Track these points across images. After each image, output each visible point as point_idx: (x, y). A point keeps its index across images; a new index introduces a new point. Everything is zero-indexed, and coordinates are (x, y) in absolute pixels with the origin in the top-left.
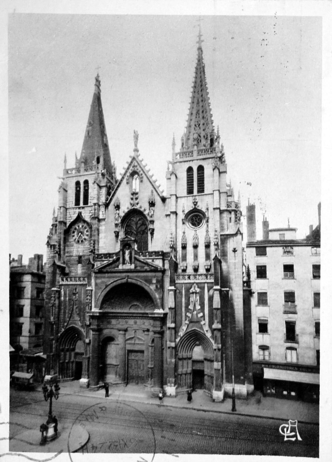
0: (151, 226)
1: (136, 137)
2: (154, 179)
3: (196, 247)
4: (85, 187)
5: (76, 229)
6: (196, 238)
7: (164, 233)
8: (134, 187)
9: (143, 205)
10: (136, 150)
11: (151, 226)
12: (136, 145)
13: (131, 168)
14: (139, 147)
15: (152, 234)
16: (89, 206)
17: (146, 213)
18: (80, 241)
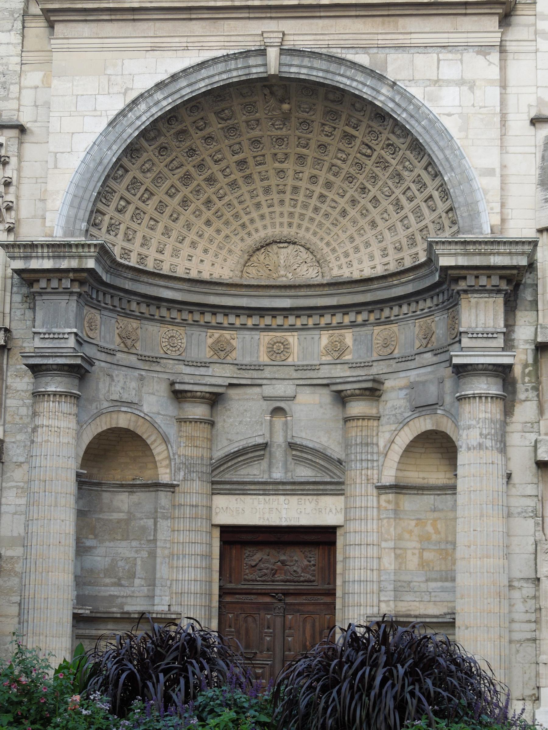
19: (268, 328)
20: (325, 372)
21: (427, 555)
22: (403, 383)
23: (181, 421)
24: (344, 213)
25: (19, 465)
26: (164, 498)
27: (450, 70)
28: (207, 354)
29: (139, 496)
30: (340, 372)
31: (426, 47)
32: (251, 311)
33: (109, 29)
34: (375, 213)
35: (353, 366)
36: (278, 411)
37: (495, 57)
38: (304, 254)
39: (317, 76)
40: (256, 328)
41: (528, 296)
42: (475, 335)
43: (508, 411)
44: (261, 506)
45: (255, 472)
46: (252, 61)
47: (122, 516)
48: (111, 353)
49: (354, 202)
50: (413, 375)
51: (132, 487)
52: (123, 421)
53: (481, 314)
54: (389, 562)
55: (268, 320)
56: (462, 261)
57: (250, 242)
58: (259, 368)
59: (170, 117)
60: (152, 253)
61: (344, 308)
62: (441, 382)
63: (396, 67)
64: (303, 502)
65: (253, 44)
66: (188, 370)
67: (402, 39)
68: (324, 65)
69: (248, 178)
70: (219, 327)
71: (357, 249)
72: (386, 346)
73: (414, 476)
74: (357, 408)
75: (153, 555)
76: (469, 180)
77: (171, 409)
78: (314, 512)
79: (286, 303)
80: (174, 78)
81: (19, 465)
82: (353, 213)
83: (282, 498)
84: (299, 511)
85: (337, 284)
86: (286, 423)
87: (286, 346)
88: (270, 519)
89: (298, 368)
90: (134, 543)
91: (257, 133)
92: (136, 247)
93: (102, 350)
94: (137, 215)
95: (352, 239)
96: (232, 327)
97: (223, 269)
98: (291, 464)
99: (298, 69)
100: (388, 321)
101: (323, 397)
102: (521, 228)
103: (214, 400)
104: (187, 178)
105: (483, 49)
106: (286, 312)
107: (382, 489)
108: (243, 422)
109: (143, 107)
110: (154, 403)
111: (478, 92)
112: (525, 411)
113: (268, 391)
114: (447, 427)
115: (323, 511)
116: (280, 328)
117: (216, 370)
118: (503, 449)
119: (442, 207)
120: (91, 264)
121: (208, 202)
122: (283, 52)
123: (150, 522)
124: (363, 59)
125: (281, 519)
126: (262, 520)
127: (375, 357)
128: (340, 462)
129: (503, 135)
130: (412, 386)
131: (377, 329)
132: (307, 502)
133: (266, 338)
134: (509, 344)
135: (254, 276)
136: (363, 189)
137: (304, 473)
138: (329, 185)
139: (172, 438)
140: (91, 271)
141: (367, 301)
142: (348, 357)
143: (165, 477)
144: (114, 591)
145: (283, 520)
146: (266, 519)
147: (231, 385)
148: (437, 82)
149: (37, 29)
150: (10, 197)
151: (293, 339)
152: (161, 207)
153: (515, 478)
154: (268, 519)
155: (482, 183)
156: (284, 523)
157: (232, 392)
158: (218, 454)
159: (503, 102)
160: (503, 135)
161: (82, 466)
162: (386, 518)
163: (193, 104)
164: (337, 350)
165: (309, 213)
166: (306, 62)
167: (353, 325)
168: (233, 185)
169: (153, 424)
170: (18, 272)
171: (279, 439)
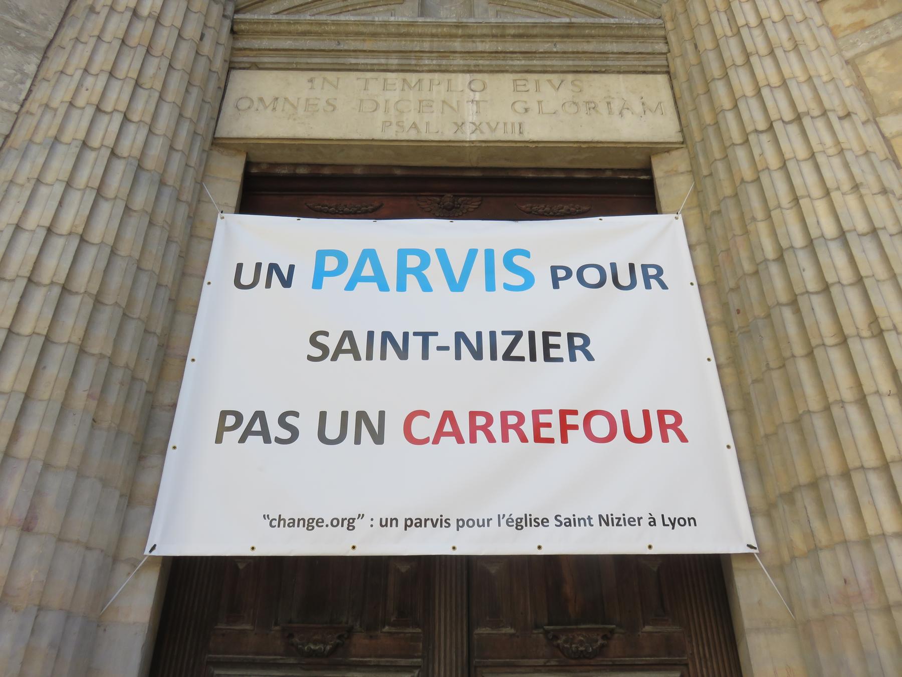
44: (394, 96)
64: (531, 86)
78: (573, 109)
83: (461, 80)
84: (519, 107)
88: (423, 128)
98: (486, 11)
115: (602, 107)
125: (460, 126)
126: (394, 128)
132: (547, 89)
145: (468, 128)
146: (407, 125)
154: (415, 126)
156: (469, 135)
162: (874, 49)
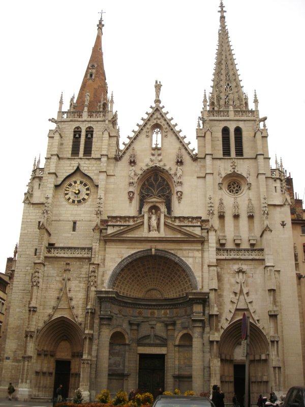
0: (179, 189)
1: (158, 87)
2: (181, 135)
3: (236, 217)
4: (87, 135)
5: (70, 185)
6: (236, 206)
7: (194, 197)
8: (154, 142)
9: (168, 164)
10: (158, 101)
11: (179, 189)
12: (158, 95)
13: (152, 120)
14: (160, 98)
15: (180, 198)
16: (93, 158)
17: (172, 172)
18: (76, 202)
19: (150, 309)
20: (162, 319)
21: (185, 361)
22: (180, 322)
23: (131, 330)
24: (167, 284)
25: (96, 339)
26: (127, 348)
27: (191, 255)
28: (137, 315)
29: (122, 347)
30: (165, 319)
31: (185, 250)
32: (147, 305)
33: (118, 244)
34: (174, 284)
35: (169, 318)
36: (152, 328)
37: (200, 252)
38: (158, 292)
39: (163, 255)
40: (147, 309)
41: (207, 303)
42: (196, 313)
43: (204, 330)
45: (147, 341)
46: (149, 252)
47: (116, 351)
48: (117, 314)
49: (170, 281)
50: (183, 320)
51: (120, 345)
52: (119, 330)
53: (198, 308)
54: (177, 363)
55: (150, 307)
56: (194, 297)
57: (146, 290)
58: (148, 318)
59: (131, 263)
60: (126, 292)
61: (167, 305)
62: (189, 322)
63: (179, 254)
65: (149, 248)
66: (133, 318)
67: (181, 248)
68: (164, 253)
69: (147, 276)
70: (140, 308)
71: (170, 292)
72: (176, 313)
73: (182, 343)
74: (170, 328)
75: (124, 360)
76: (195, 278)
77: (129, 327)
79: (154, 303)
80: (132, 255)
81: (96, 339)
82: (169, 283)
85: (166, 300)
86: (154, 331)
87: (154, 313)
89: (157, 318)
90: (120, 358)
91: (149, 266)
92: (122, 291)
93: (115, 314)
94: (123, 283)
95: (169, 289)
96: (142, 308)
97: (140, 295)
99: (159, 254)
100: (177, 308)
101: (163, 324)
102: (206, 290)
103: (138, 325)
104: (133, 276)
105: (198, 250)
106: (154, 305)
107: (175, 346)
108: (145, 330)
109: (125, 261)
110: (125, 325)
111: (197, 260)
112: (207, 329)
113: (151, 323)
114: (190, 332)
116: (153, 309)
117: (139, 318)
118: (202, 338)
119: (189, 284)
120: (114, 296)
121: (138, 281)
122: (155, 250)
123: (124, 353)
124: (173, 252)
127: (174, 315)
128: (166, 339)
129: (202, 269)
130: (182, 323)
131: (174, 310)
133: (150, 311)
134: (204, 314)
135: (147, 297)
136: (172, 279)
137: (158, 342)
138: (164, 278)
139: (129, 334)
140: (114, 297)
141: (173, 304)
142: (168, 316)
143: (127, 342)
144: (115, 368)
147: (142, 322)
148: (188, 257)
149: (102, 243)
150: (96, 280)
151: (156, 311)
152: (128, 281)
153: (205, 344)
155: (198, 279)
157: (143, 323)
158: (139, 337)
159: (202, 262)
160: (202, 269)
161: (111, 339)
163: (136, 260)
164: (165, 314)
165: (160, 283)
166: (160, 252)
167: (169, 309)
168: (143, 277)
169: (125, 330)
170: (98, 297)
171: (153, 334)
